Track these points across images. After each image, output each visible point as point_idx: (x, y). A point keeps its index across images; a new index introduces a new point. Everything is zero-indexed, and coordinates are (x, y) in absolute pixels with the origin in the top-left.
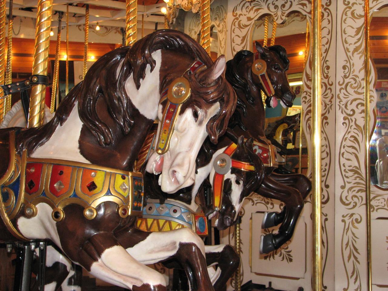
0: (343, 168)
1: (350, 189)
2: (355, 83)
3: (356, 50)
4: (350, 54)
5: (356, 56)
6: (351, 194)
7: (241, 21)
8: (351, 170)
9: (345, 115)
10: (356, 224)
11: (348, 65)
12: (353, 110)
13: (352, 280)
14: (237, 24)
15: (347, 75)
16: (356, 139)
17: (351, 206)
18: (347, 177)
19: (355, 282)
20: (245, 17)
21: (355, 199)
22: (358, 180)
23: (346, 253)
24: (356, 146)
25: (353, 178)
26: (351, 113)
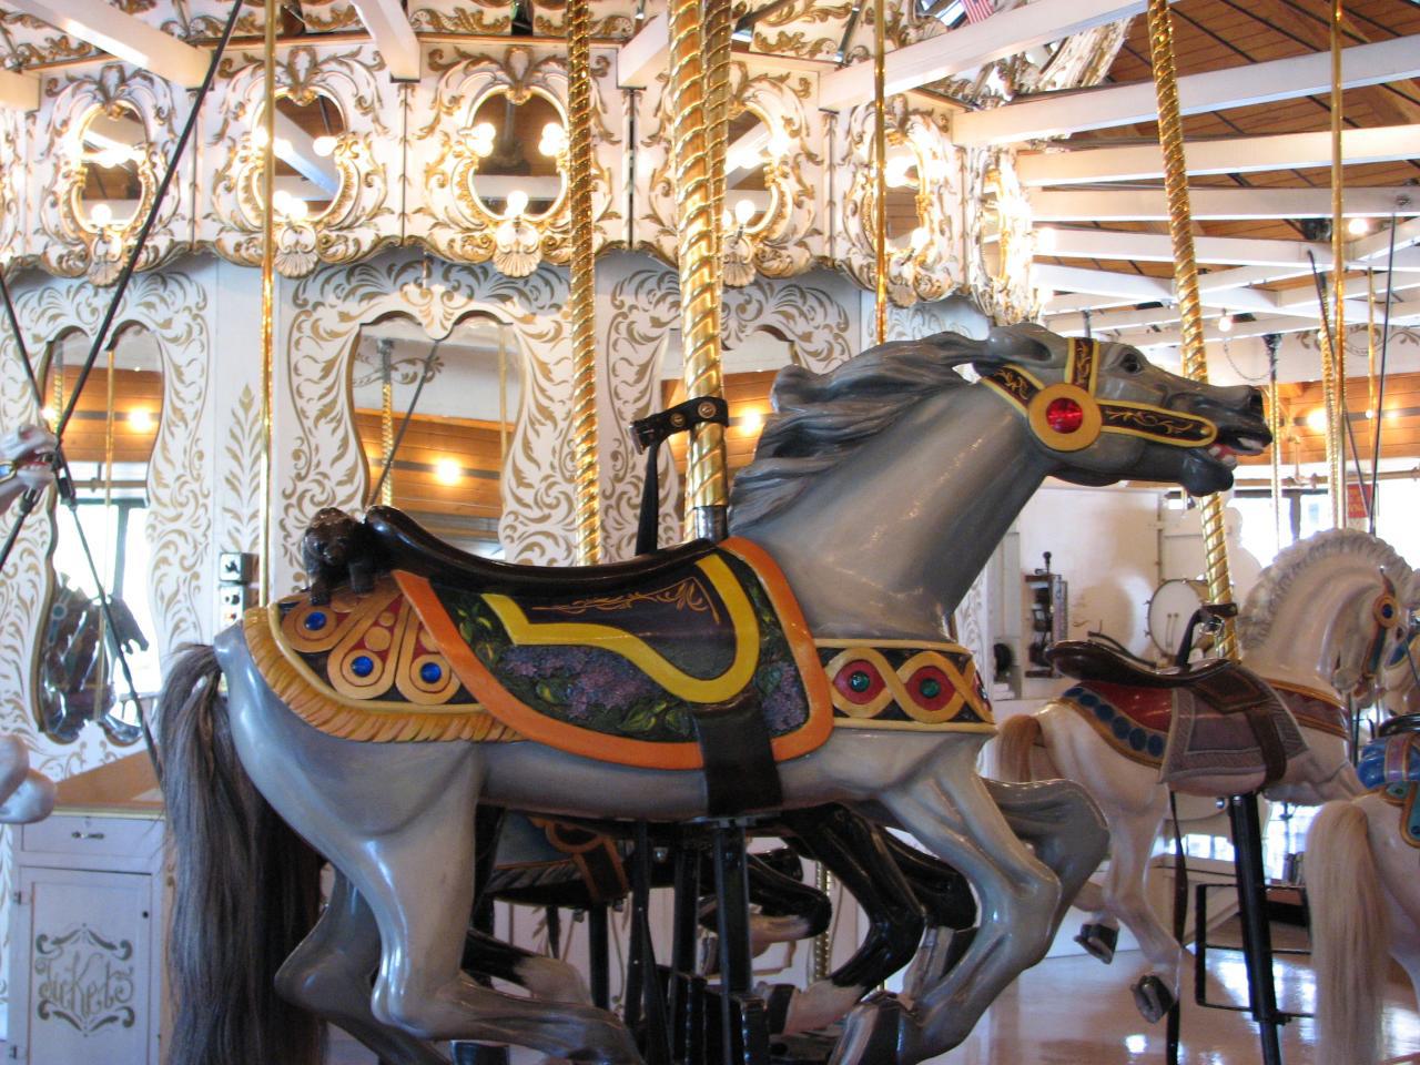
2: (323, 493)
3: (323, 413)
5: (325, 427)
7: (633, 322)
8: (8, 701)
11: (305, 448)
14: (623, 328)
15: (303, 472)
16: (18, 630)
20: (646, 317)
22: (20, 724)
25: (12, 717)
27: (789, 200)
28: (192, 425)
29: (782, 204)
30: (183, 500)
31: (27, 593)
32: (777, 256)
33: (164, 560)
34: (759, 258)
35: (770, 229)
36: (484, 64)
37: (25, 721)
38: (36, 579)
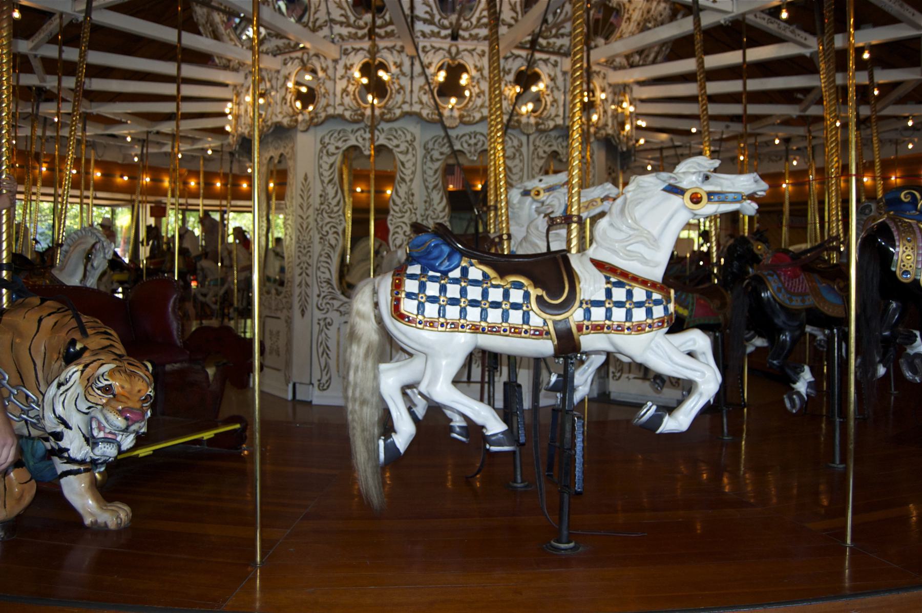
0: (319, 280)
1: (324, 297)
4: (325, 185)
6: (325, 301)
8: (325, 282)
9: (321, 235)
10: (328, 327)
12: (327, 232)
13: (324, 373)
17: (324, 311)
18: (322, 287)
19: (327, 374)
21: (328, 306)
23: (321, 350)
24: (329, 261)
26: (325, 234)
27: (549, 103)
28: (409, 184)
29: (546, 105)
30: (404, 210)
31: (333, 242)
32: (543, 123)
33: (397, 232)
34: (537, 124)
35: (542, 113)
36: (361, 52)
37: (333, 289)
38: (337, 237)
